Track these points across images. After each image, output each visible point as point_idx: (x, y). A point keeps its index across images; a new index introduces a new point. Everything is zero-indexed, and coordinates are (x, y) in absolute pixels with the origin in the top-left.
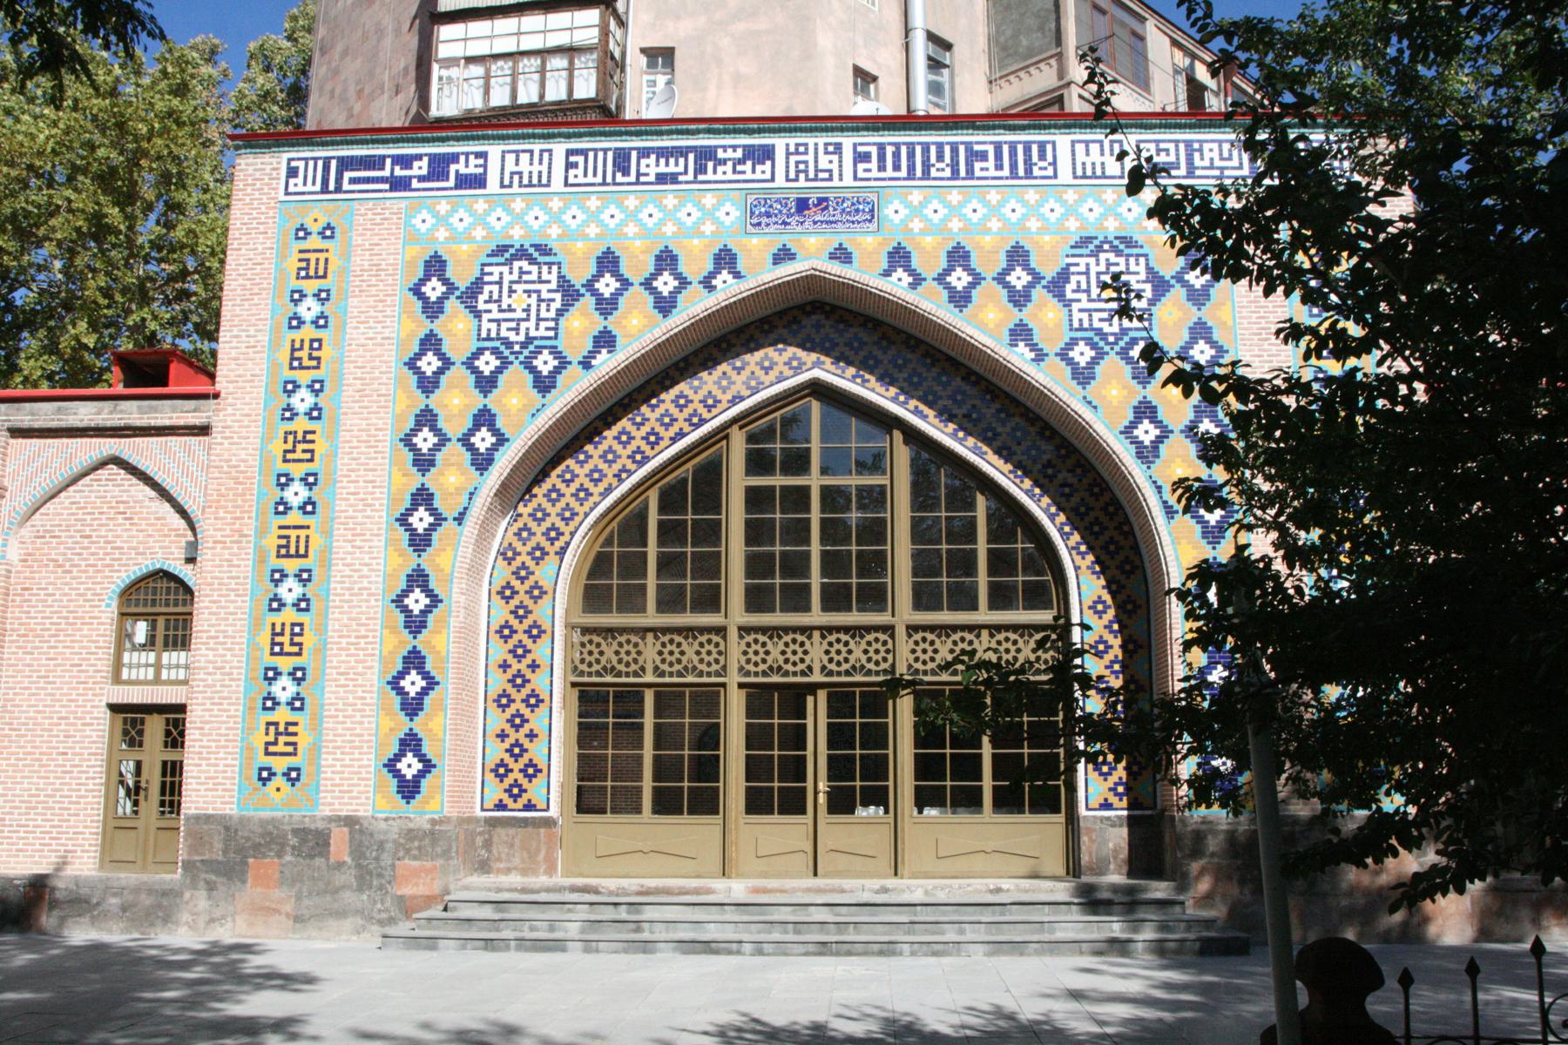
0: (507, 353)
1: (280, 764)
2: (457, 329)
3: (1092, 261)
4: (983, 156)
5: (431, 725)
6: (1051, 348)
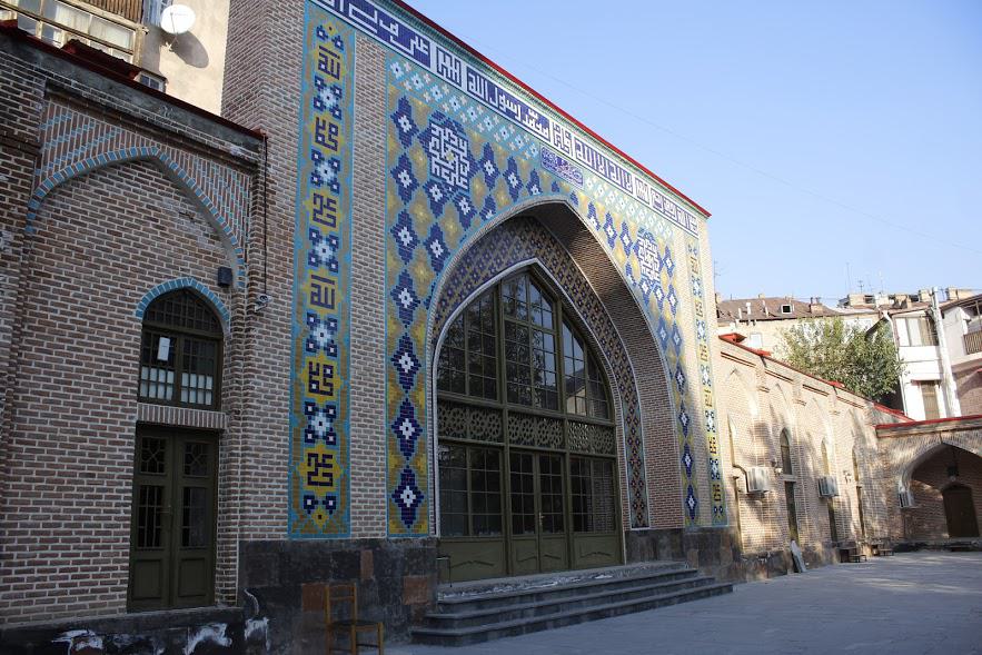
1: (320, 493)
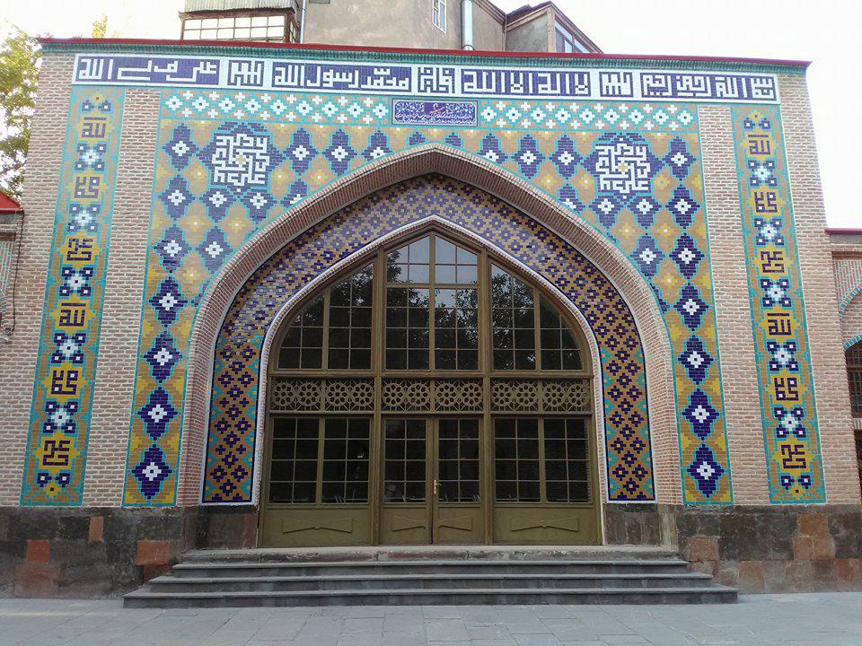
0: (232, 193)
1: (54, 471)
2: (197, 174)
3: (612, 148)
4: (544, 81)
5: (169, 442)
6: (587, 202)
